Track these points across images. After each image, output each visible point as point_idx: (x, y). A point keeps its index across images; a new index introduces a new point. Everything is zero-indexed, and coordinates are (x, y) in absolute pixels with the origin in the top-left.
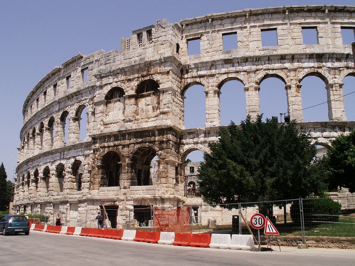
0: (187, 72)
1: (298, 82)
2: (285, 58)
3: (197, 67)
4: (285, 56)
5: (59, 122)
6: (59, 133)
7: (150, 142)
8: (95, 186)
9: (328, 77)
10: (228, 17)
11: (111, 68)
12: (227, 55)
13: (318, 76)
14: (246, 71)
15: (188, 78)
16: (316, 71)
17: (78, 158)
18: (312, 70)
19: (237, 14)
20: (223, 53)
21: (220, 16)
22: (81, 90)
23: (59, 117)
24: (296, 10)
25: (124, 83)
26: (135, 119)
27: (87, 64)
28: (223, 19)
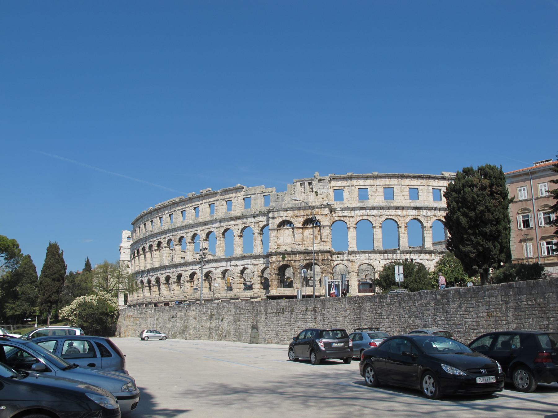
0: (335, 213)
3: (342, 209)
5: (221, 237)
6: (222, 245)
7: (316, 260)
8: (273, 287)
10: (362, 177)
11: (281, 205)
12: (362, 204)
17: (246, 266)
19: (369, 176)
20: (359, 202)
22: (247, 215)
23: (221, 232)
25: (293, 218)
26: (303, 244)
27: (250, 195)
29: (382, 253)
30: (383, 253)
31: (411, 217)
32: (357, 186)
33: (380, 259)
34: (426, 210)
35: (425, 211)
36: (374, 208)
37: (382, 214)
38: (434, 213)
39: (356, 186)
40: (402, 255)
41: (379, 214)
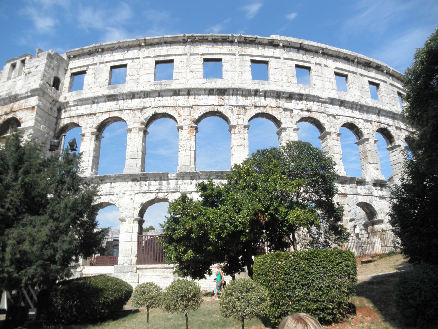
0: (65, 112)
1: (192, 122)
2: (179, 93)
4: (179, 91)
9: (231, 117)
13: (221, 117)
14: (131, 109)
15: (65, 118)
16: (216, 110)
18: (211, 109)
19: (130, 44)
20: (108, 88)
21: (110, 46)
24: (199, 39)
28: (114, 50)
29: (138, 179)
30: (141, 180)
31: (204, 110)
32: (109, 62)
33: (132, 193)
34: (237, 95)
35: (234, 97)
36: (132, 96)
37: (146, 105)
38: (253, 101)
39: (107, 62)
40: (180, 182)
41: (141, 105)
